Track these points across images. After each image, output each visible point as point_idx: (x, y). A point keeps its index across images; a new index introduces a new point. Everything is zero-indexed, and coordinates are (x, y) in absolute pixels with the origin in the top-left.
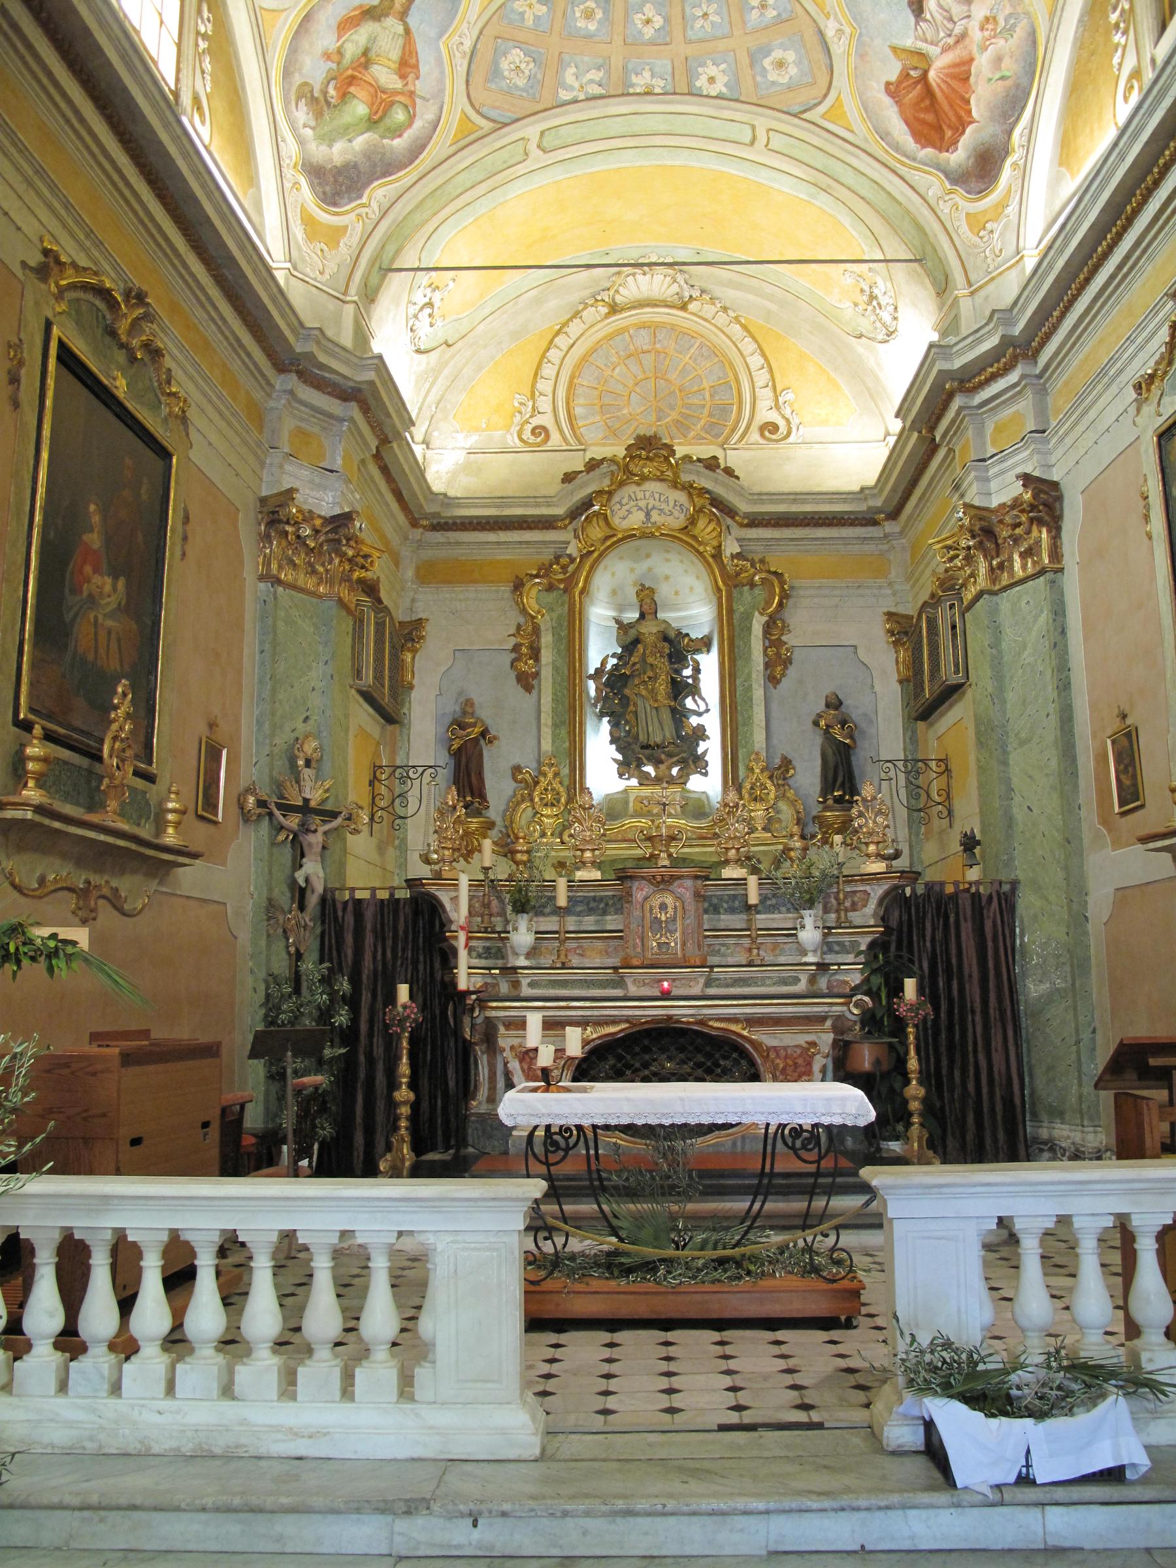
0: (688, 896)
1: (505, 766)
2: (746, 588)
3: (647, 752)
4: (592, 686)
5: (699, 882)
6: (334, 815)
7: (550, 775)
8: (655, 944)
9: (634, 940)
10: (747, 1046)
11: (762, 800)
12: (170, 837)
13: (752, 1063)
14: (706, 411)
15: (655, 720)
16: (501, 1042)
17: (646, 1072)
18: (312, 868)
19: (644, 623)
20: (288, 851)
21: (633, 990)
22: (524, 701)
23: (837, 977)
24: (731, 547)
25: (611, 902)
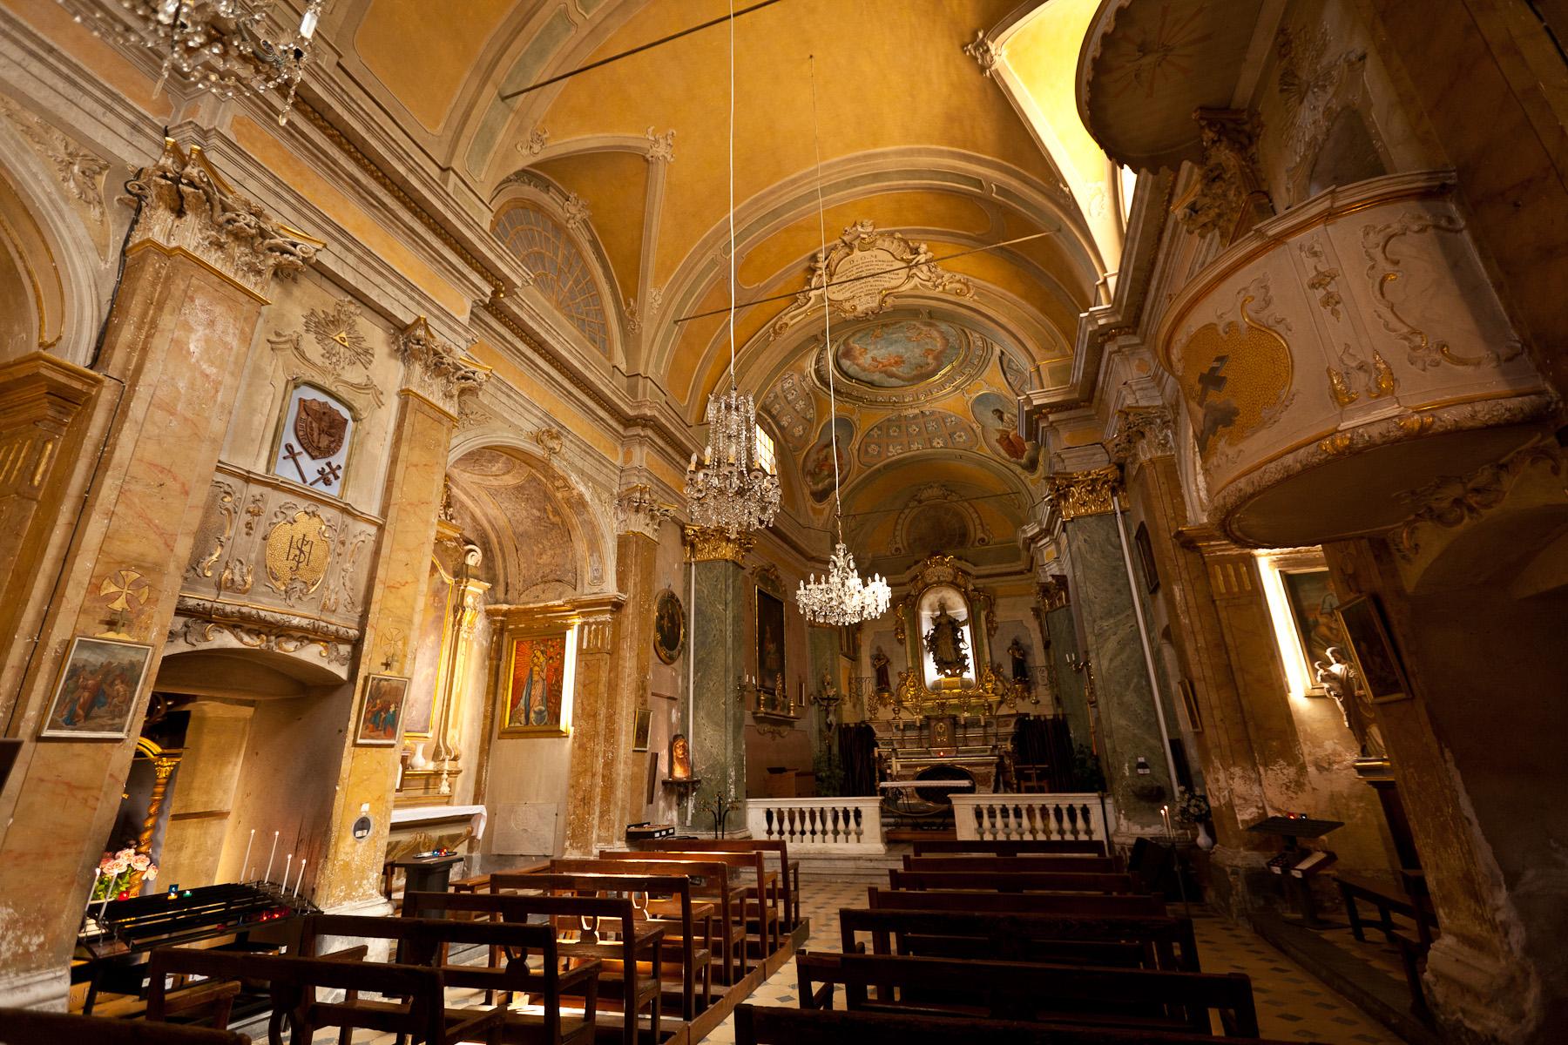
1: (896, 672)
4: (925, 642)
6: (837, 699)
12: (792, 714)
18: (832, 718)
20: (824, 714)
21: (933, 755)
22: (902, 650)
24: (971, 587)
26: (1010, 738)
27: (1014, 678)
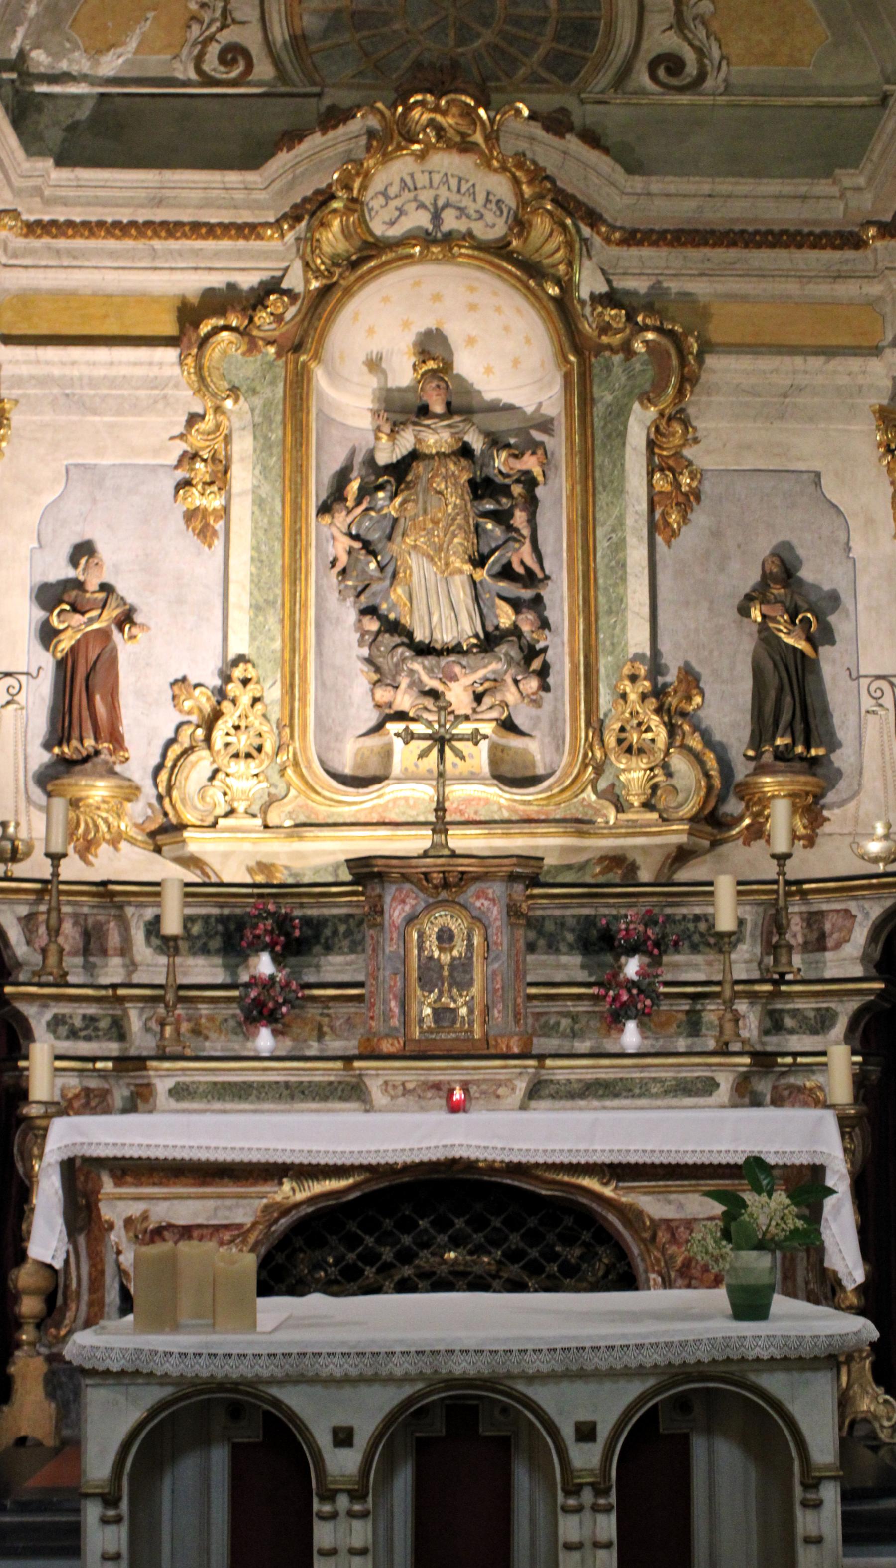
0: (495, 913)
2: (618, 358)
5: (519, 887)
7: (245, 700)
8: (427, 1011)
9: (386, 1002)
10: (612, 1218)
11: (641, 751)
13: (621, 1253)
14: (549, 30)
16: (106, 1212)
17: (407, 1271)
23: (792, 1080)
25: (342, 929)
26: (845, 1009)
27: (758, 738)
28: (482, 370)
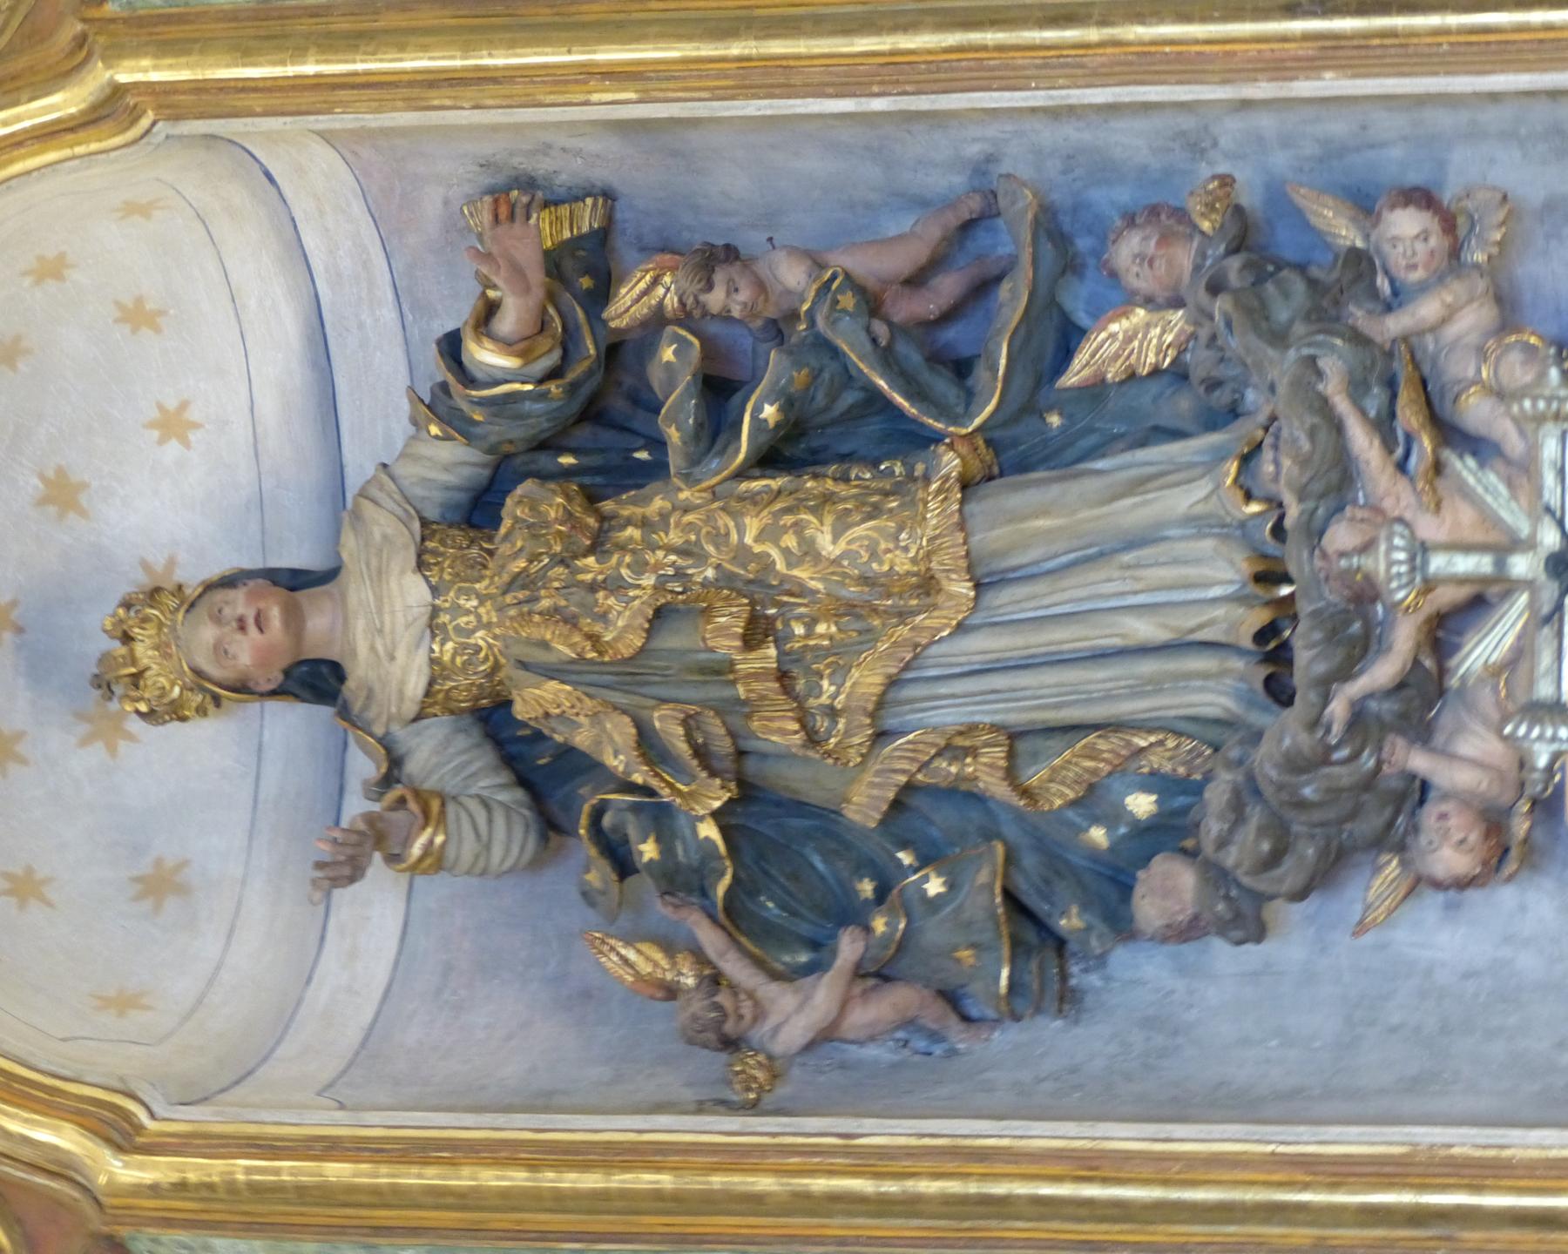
3: (1308, 660)
15: (1010, 609)
19: (360, 671)
28: (173, 448)
